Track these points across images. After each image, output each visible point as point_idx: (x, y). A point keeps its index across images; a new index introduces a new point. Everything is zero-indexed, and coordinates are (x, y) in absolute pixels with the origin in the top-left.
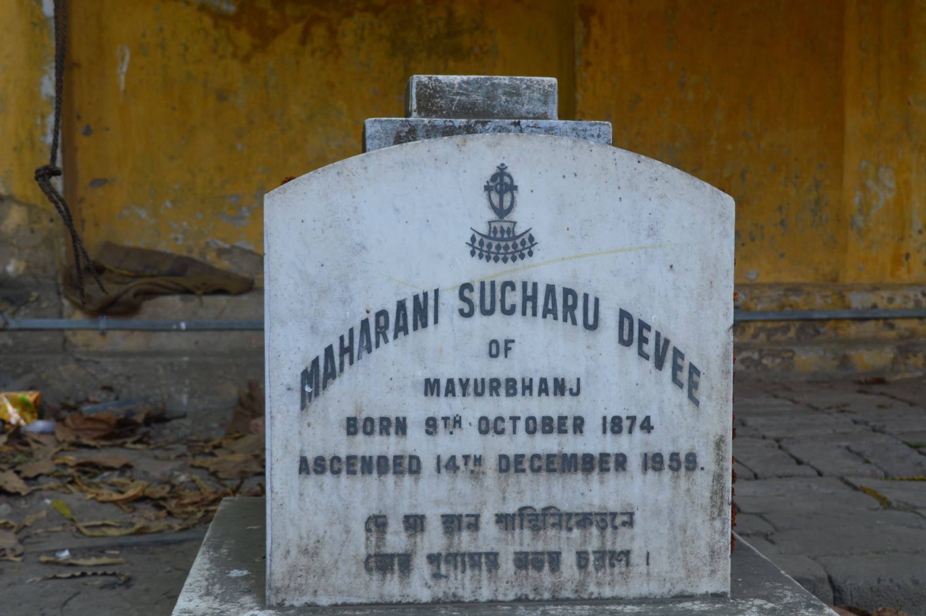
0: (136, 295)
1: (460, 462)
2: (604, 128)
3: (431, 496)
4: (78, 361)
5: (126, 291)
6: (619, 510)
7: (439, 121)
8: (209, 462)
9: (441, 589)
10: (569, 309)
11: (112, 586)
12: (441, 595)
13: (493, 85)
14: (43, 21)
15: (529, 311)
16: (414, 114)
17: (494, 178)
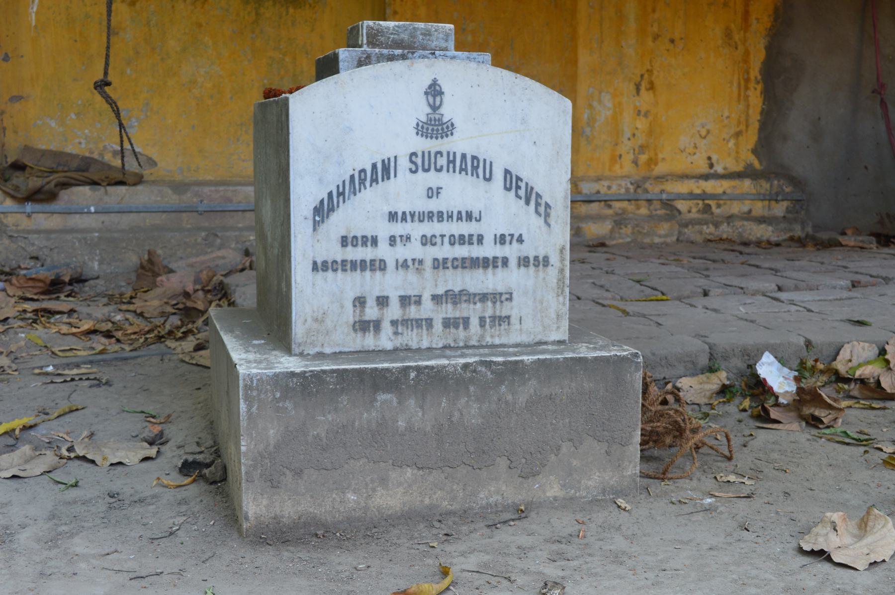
0: (56, 185)
1: (410, 263)
2: (486, 57)
3: (392, 284)
4: (11, 236)
5: (48, 183)
6: (503, 291)
7: (385, 51)
8: (131, 307)
9: (399, 342)
10: (475, 168)
11: (98, 386)
12: (398, 345)
13: (414, 28)
15: (451, 169)
16: (365, 46)
17: (430, 87)
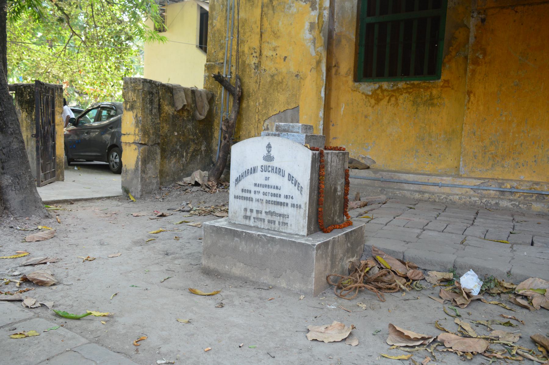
3: (254, 206)
9: (255, 224)
10: (280, 172)
14: (321, 98)
